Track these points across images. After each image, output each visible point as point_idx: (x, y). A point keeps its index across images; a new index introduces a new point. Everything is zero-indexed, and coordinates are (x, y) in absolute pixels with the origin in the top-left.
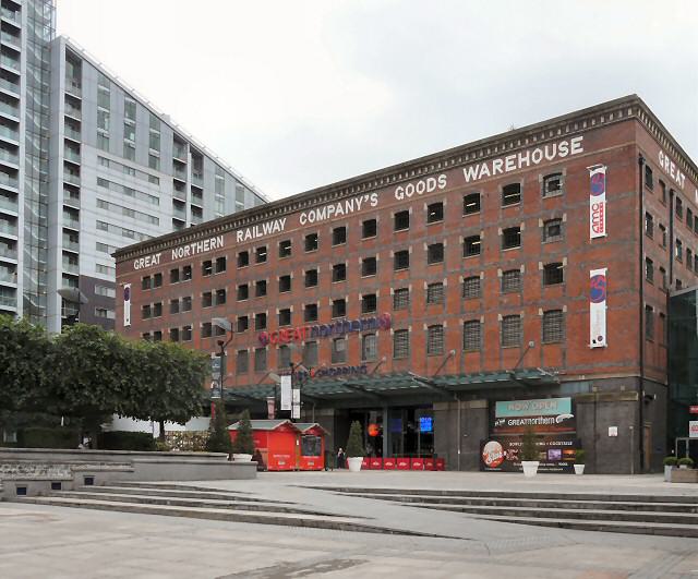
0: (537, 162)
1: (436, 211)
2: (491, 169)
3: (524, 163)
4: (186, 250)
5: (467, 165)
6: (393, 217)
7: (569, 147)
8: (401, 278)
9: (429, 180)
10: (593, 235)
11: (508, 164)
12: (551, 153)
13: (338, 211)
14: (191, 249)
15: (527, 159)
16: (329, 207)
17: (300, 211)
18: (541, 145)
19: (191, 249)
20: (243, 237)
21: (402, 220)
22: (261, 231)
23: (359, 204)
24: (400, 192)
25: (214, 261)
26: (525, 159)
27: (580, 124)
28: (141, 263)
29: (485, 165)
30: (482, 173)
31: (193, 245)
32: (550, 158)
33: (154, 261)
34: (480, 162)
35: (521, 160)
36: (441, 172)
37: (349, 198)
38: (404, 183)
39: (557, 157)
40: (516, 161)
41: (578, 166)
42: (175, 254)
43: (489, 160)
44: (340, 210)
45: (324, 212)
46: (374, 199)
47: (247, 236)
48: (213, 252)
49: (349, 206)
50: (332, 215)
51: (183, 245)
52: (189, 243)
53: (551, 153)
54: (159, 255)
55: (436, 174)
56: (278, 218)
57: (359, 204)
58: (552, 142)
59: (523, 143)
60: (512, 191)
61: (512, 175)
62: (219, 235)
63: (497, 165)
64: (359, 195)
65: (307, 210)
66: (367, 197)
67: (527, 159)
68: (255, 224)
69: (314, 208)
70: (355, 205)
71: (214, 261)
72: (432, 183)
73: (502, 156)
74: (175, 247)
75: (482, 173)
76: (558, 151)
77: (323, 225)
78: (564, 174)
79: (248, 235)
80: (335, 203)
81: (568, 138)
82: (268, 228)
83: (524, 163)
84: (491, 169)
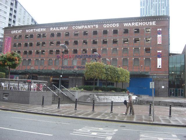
0: (144, 25)
1: (115, 32)
2: (131, 24)
3: (140, 25)
4: (32, 30)
5: (125, 23)
6: (102, 31)
7: (152, 23)
8: (105, 46)
9: (114, 24)
10: (158, 43)
11: (136, 24)
12: (147, 24)
13: (85, 27)
14: (33, 30)
15: (141, 24)
16: (82, 26)
17: (73, 26)
18: (145, 22)
19: (33, 30)
20: (53, 29)
21: (105, 32)
22: (59, 28)
23: (92, 27)
24: (105, 26)
25: (42, 34)
26: (141, 24)
27: (155, 19)
28: (14, 32)
29: (130, 23)
30: (129, 25)
31: (34, 29)
32: (147, 25)
33: (19, 32)
34: (129, 22)
35: (140, 24)
36: (117, 23)
37: (89, 25)
38: (106, 24)
39: (149, 25)
40: (138, 24)
41: (154, 28)
42: (27, 31)
43: (131, 22)
44: (86, 27)
45: (81, 27)
46: (97, 26)
47: (54, 29)
48: (41, 32)
49: (89, 27)
50: (83, 28)
51: (31, 29)
52: (33, 29)
53: (147, 24)
54: (21, 30)
55: (116, 23)
56: (65, 26)
57: (92, 27)
58: (148, 21)
59: (140, 20)
60: (137, 31)
61: (137, 27)
62: (44, 28)
63: (133, 24)
64: (92, 25)
65: (75, 26)
66: (95, 25)
67: (141, 24)
68: (57, 27)
69: (78, 26)
70: (91, 27)
71: (42, 34)
72: (114, 25)
73: (135, 22)
74: (27, 29)
75: (129, 25)
76: (149, 24)
77: (80, 30)
78: (151, 29)
79: (54, 29)
80: (85, 25)
81: (152, 21)
82: (61, 28)
83: (140, 25)
84: (131, 24)
